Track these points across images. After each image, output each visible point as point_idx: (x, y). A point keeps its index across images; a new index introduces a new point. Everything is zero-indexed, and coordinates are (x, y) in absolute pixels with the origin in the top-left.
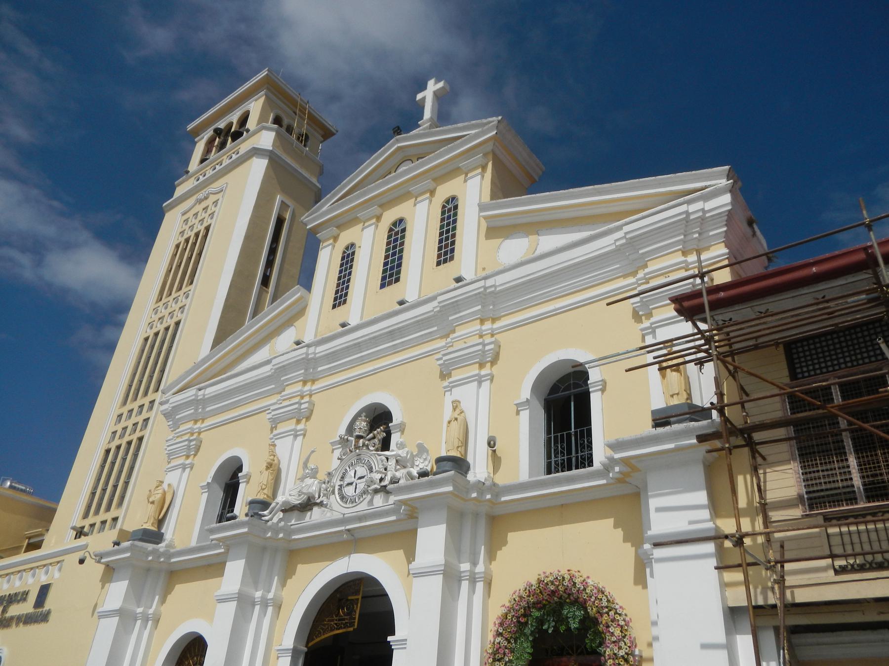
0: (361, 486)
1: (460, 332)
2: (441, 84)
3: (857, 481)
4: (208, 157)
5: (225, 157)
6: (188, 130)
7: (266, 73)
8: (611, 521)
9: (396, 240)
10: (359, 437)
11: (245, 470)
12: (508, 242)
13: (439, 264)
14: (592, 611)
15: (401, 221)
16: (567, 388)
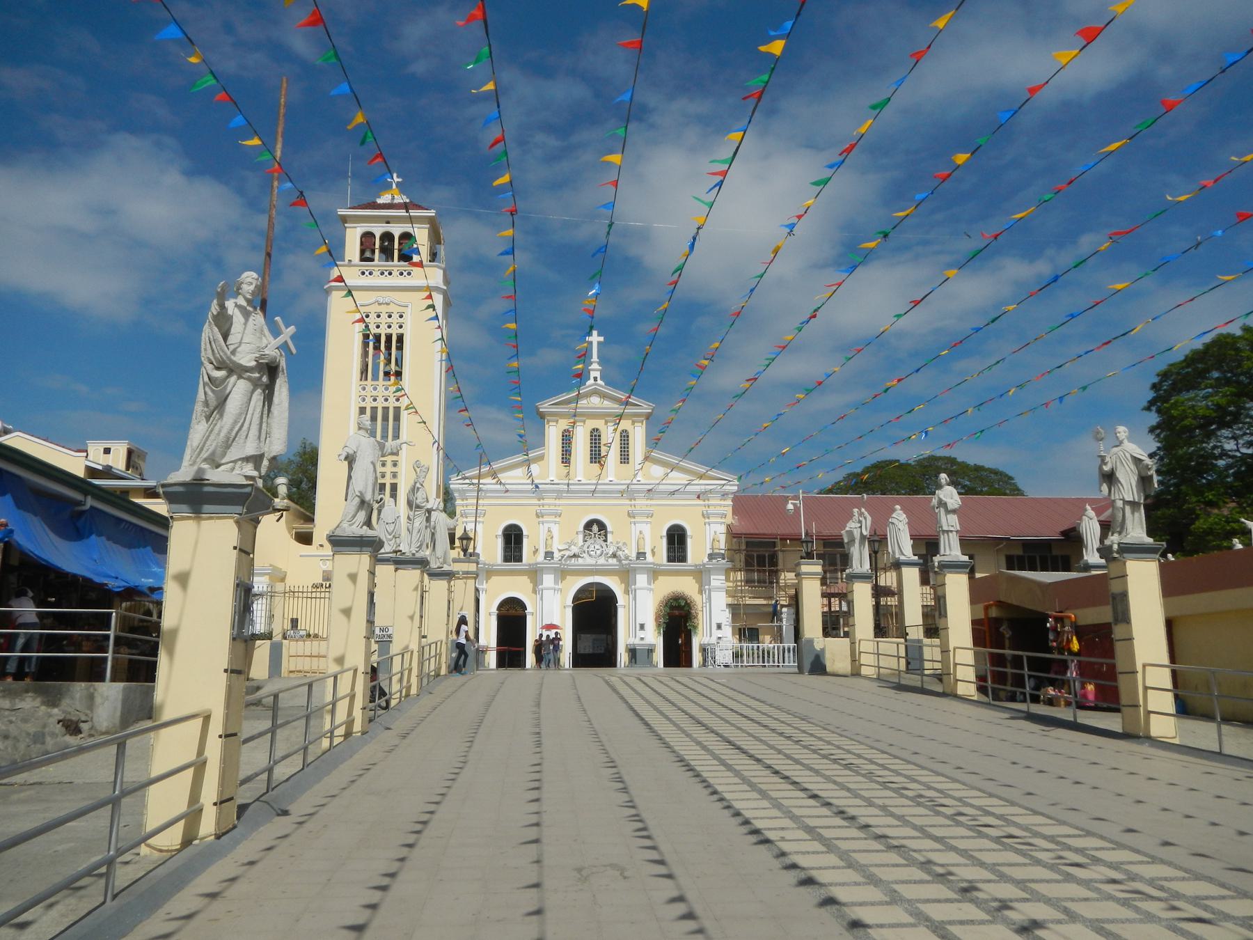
0: (598, 552)
1: (637, 502)
2: (601, 339)
3: (756, 578)
4: (368, 254)
5: (396, 269)
6: (339, 213)
7: (434, 214)
8: (692, 577)
9: (595, 440)
10: (595, 534)
11: (524, 534)
12: (654, 466)
13: (621, 463)
14: (689, 601)
15: (597, 430)
16: (674, 531)
